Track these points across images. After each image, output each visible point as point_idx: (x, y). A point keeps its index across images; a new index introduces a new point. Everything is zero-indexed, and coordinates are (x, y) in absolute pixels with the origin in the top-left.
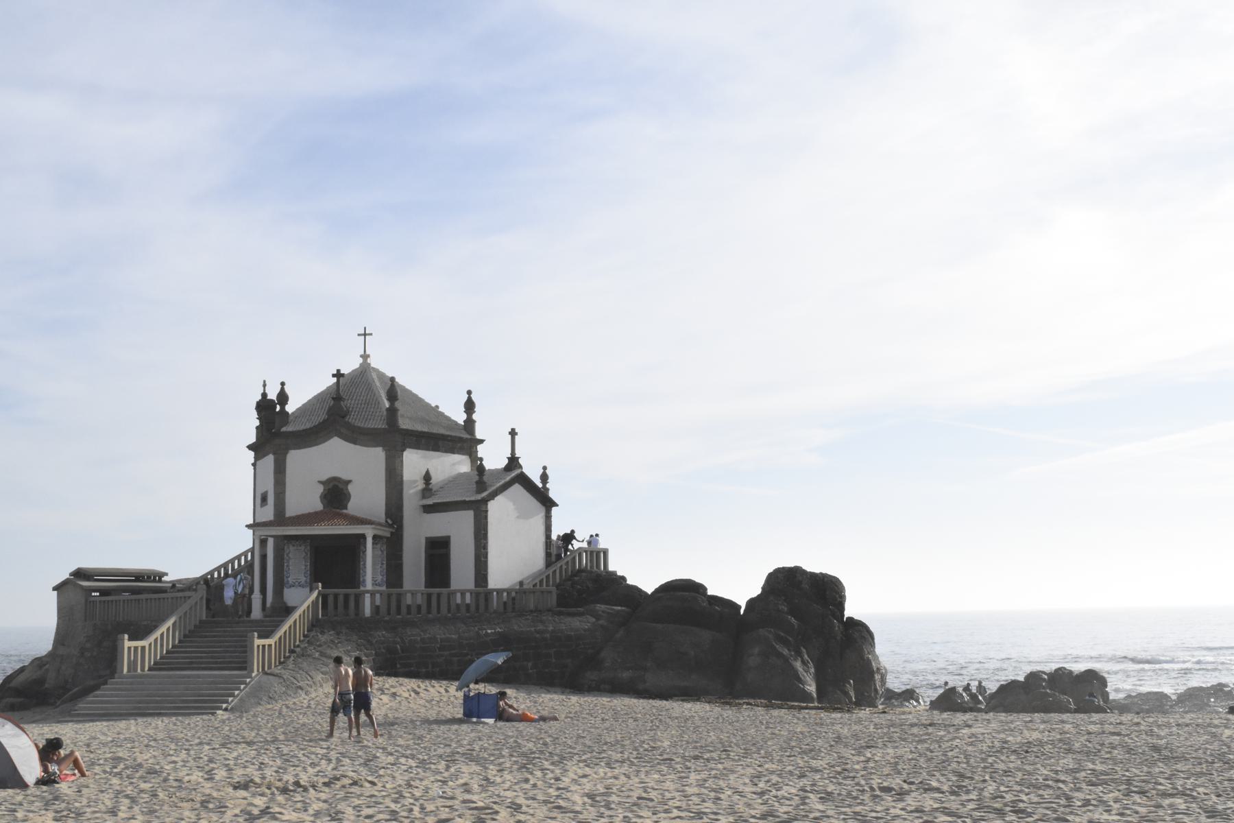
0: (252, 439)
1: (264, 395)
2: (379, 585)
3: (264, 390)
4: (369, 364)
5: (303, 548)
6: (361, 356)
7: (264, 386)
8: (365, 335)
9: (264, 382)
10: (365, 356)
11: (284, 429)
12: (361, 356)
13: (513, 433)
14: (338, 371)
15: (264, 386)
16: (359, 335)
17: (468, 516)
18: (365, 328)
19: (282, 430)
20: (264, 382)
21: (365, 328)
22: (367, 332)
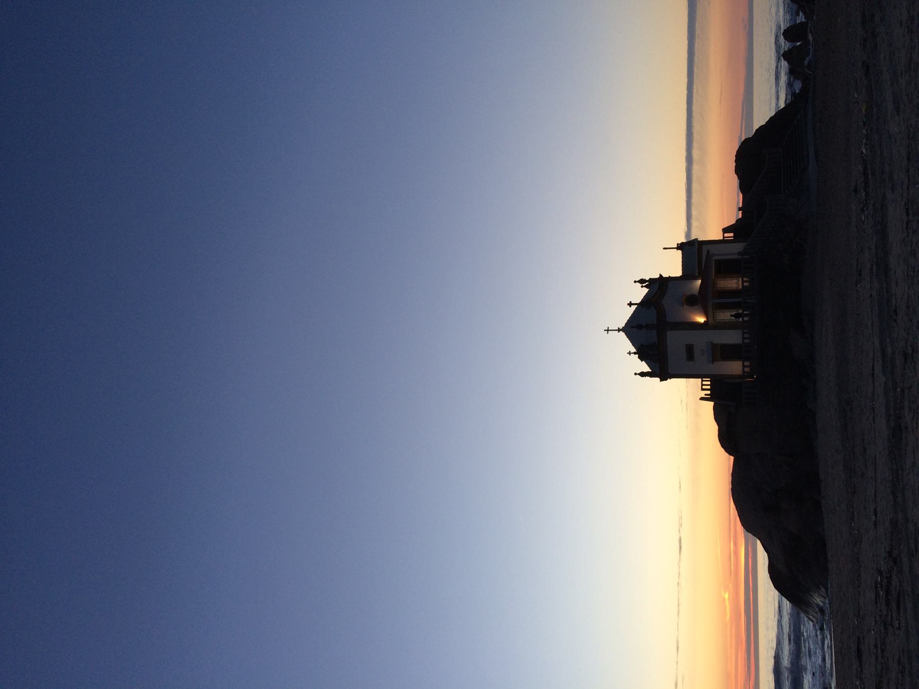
0: (658, 379)
1: (635, 353)
2: (739, 280)
3: (632, 353)
4: (623, 327)
5: (718, 314)
6: (619, 332)
7: (630, 353)
8: (608, 330)
9: (628, 353)
10: (619, 330)
11: (655, 323)
12: (619, 332)
13: (664, 249)
14: (628, 304)
15: (630, 353)
16: (608, 333)
17: (704, 246)
18: (605, 330)
19: (655, 323)
20: (628, 353)
21: (605, 330)
22: (607, 329)
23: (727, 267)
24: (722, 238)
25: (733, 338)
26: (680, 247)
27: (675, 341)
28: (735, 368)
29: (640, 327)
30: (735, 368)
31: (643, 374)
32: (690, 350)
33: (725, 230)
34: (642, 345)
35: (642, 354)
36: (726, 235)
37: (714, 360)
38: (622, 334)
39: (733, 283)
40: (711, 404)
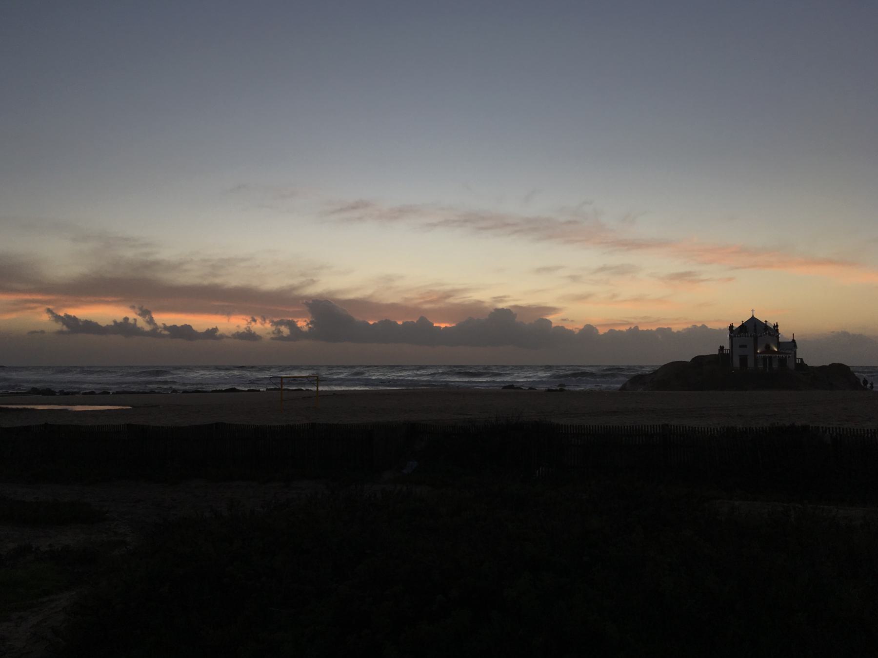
8: (753, 311)
10: (753, 315)
23: (783, 361)
24: (797, 357)
25: (751, 363)
26: (794, 341)
29: (755, 326)
32: (745, 346)
33: (802, 360)
34: (746, 327)
35: (744, 327)
36: (800, 360)
37: (740, 356)
38: (751, 316)
39: (775, 365)
40: (717, 353)
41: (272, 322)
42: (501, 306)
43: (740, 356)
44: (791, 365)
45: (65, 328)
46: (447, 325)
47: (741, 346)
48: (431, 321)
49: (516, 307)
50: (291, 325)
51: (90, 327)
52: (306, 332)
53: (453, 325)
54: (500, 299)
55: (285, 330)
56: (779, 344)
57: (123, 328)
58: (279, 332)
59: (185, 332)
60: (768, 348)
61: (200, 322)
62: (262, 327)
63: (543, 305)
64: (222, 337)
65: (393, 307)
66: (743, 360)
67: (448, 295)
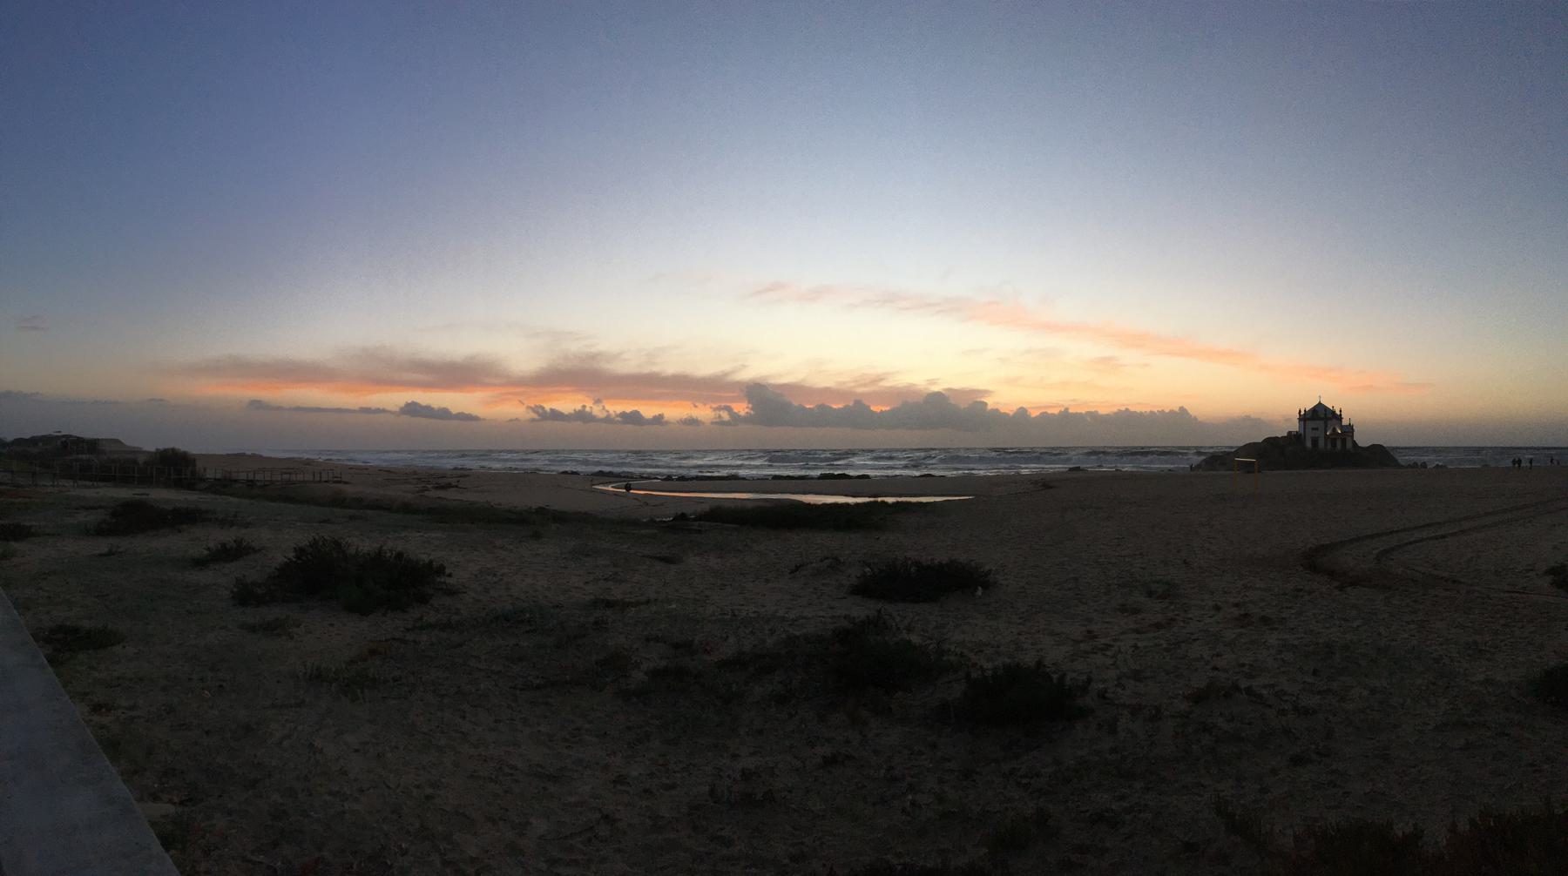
23: (1344, 442)
25: (1321, 443)
27: (1321, 424)
28: (1309, 444)
29: (1326, 411)
30: (1309, 444)
31: (1300, 411)
32: (1317, 429)
39: (1339, 443)
41: (711, 408)
42: (935, 389)
43: (1312, 438)
44: (1349, 445)
45: (536, 416)
46: (884, 409)
47: (1313, 429)
48: (867, 403)
49: (949, 390)
50: (728, 409)
51: (556, 415)
52: (729, 421)
53: (888, 408)
54: (932, 382)
55: (725, 416)
56: (1342, 427)
57: (582, 416)
58: (720, 416)
59: (634, 418)
60: (1334, 429)
61: (648, 411)
62: (704, 413)
63: (975, 388)
64: (667, 423)
65: (826, 391)
66: (1315, 441)
67: (880, 379)
